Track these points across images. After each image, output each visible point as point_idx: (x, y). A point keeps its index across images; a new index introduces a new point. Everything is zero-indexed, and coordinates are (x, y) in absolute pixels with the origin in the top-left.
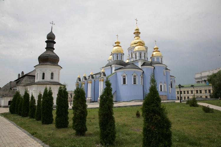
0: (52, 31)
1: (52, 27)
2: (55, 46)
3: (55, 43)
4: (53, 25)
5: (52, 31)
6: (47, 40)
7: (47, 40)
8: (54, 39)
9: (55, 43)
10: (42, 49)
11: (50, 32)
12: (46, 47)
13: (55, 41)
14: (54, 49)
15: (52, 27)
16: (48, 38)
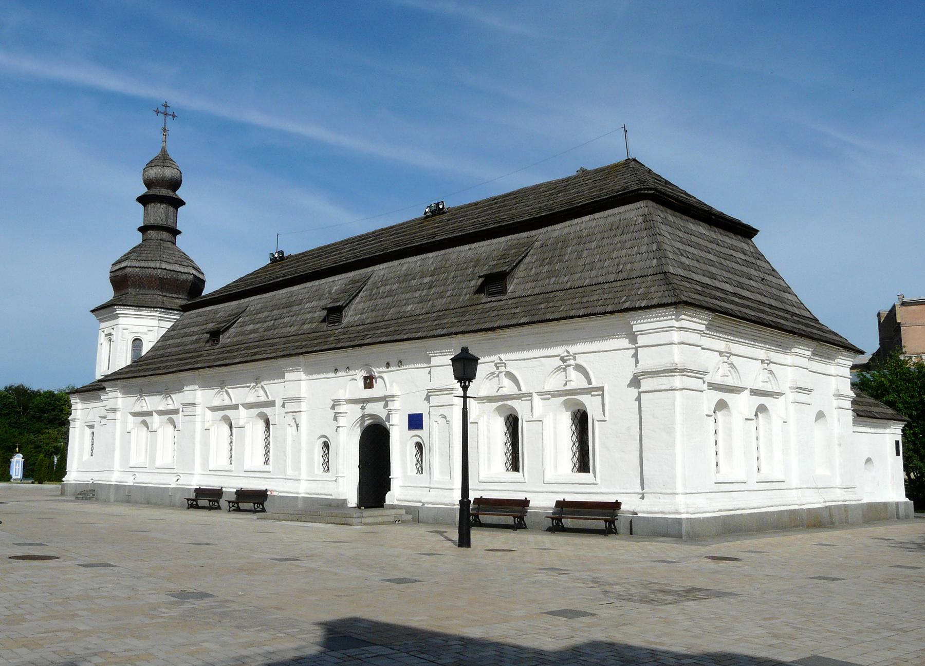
0: (164, 151)
1: (165, 130)
2: (184, 218)
3: (181, 203)
4: (169, 118)
5: (164, 151)
6: (143, 190)
7: (143, 190)
8: (175, 184)
9: (181, 203)
10: (123, 233)
11: (156, 153)
12: (142, 225)
13: (180, 193)
14: (179, 232)
15: (165, 130)
16: (149, 183)
